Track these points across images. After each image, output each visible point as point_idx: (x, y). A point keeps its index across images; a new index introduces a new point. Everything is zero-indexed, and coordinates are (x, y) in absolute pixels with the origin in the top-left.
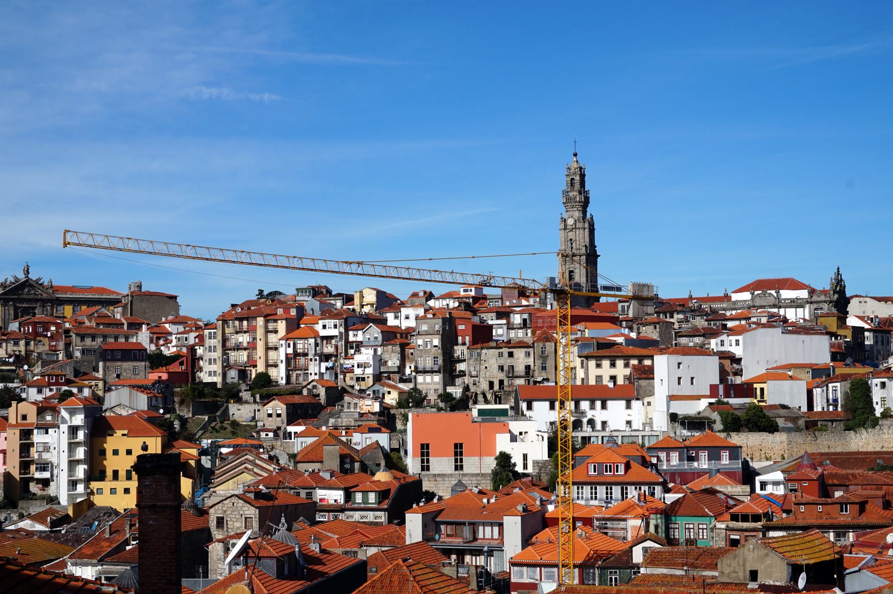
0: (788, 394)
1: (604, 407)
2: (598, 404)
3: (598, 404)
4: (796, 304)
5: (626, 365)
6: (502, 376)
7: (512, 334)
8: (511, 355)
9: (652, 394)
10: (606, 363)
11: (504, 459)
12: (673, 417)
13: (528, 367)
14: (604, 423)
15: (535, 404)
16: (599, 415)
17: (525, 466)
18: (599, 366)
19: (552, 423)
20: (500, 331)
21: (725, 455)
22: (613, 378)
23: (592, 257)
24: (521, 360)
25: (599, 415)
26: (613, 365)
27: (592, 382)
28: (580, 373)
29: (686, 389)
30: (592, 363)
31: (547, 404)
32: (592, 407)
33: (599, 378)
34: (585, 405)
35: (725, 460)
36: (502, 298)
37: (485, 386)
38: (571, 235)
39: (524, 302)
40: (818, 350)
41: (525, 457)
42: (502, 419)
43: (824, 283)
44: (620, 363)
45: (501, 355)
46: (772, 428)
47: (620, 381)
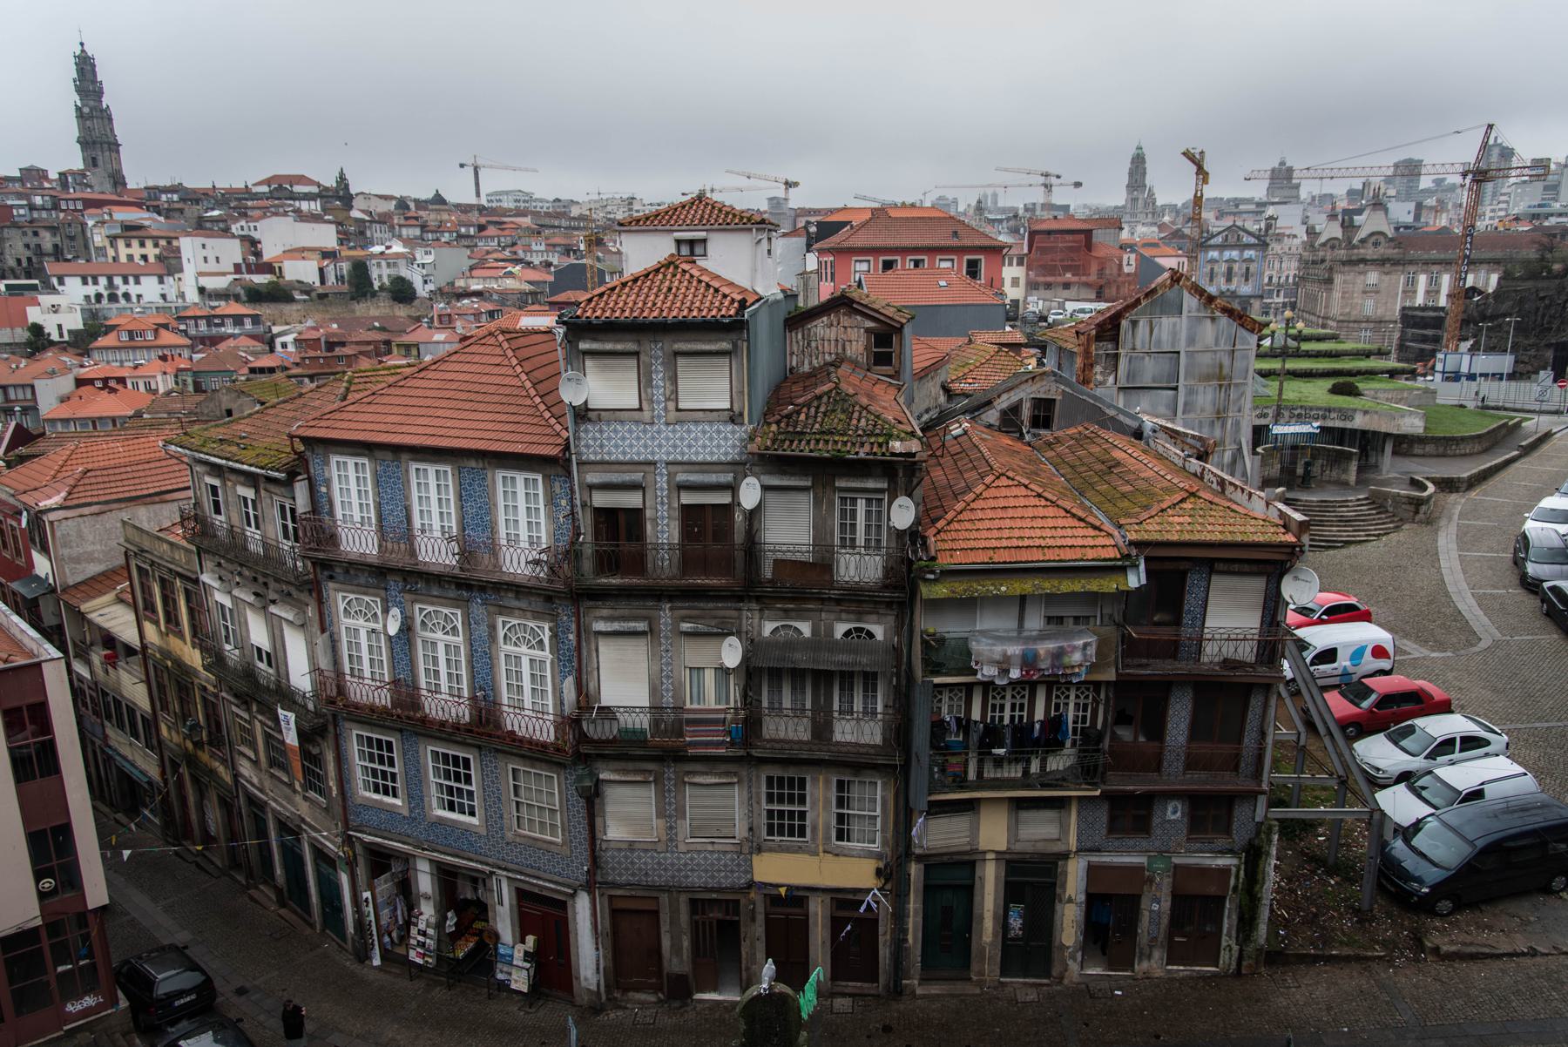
0: (303, 271)
1: (137, 282)
2: (131, 280)
3: (131, 280)
4: (308, 197)
5: (156, 245)
6: (28, 253)
7: (35, 215)
8: (36, 234)
9: (181, 270)
10: (135, 243)
11: (37, 330)
12: (202, 290)
13: (56, 246)
14: (139, 296)
15: (67, 280)
16: (133, 289)
17: (61, 335)
18: (128, 245)
19: (87, 298)
20: (22, 212)
21: (248, 321)
22: (145, 257)
23: (114, 146)
24: (47, 241)
25: (133, 289)
26: (142, 245)
27: (123, 259)
28: (111, 252)
29: (212, 266)
30: (121, 244)
31: (79, 280)
32: (126, 282)
33: (130, 257)
34: (118, 281)
35: (248, 325)
36: (21, 180)
37: (12, 263)
38: (88, 123)
39: (47, 185)
40: (326, 236)
41: (60, 327)
42: (33, 294)
43: (330, 182)
44: (149, 243)
45: (25, 234)
46: (291, 300)
47: (152, 259)
